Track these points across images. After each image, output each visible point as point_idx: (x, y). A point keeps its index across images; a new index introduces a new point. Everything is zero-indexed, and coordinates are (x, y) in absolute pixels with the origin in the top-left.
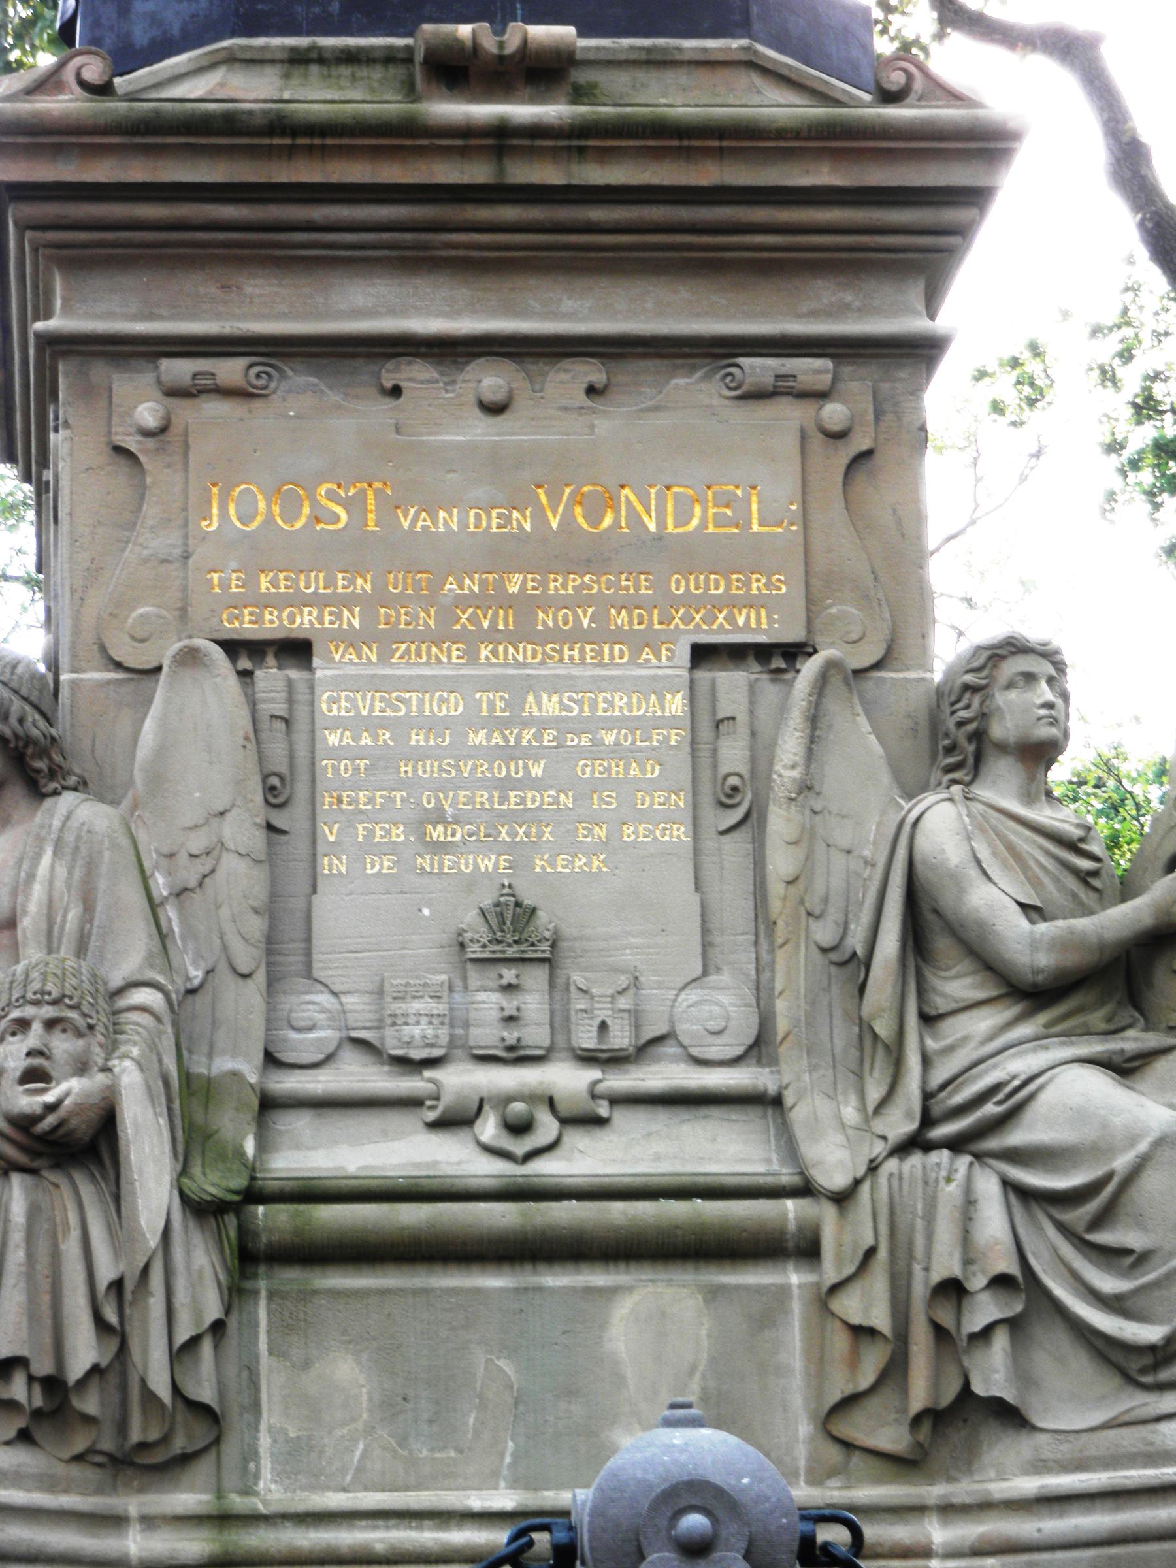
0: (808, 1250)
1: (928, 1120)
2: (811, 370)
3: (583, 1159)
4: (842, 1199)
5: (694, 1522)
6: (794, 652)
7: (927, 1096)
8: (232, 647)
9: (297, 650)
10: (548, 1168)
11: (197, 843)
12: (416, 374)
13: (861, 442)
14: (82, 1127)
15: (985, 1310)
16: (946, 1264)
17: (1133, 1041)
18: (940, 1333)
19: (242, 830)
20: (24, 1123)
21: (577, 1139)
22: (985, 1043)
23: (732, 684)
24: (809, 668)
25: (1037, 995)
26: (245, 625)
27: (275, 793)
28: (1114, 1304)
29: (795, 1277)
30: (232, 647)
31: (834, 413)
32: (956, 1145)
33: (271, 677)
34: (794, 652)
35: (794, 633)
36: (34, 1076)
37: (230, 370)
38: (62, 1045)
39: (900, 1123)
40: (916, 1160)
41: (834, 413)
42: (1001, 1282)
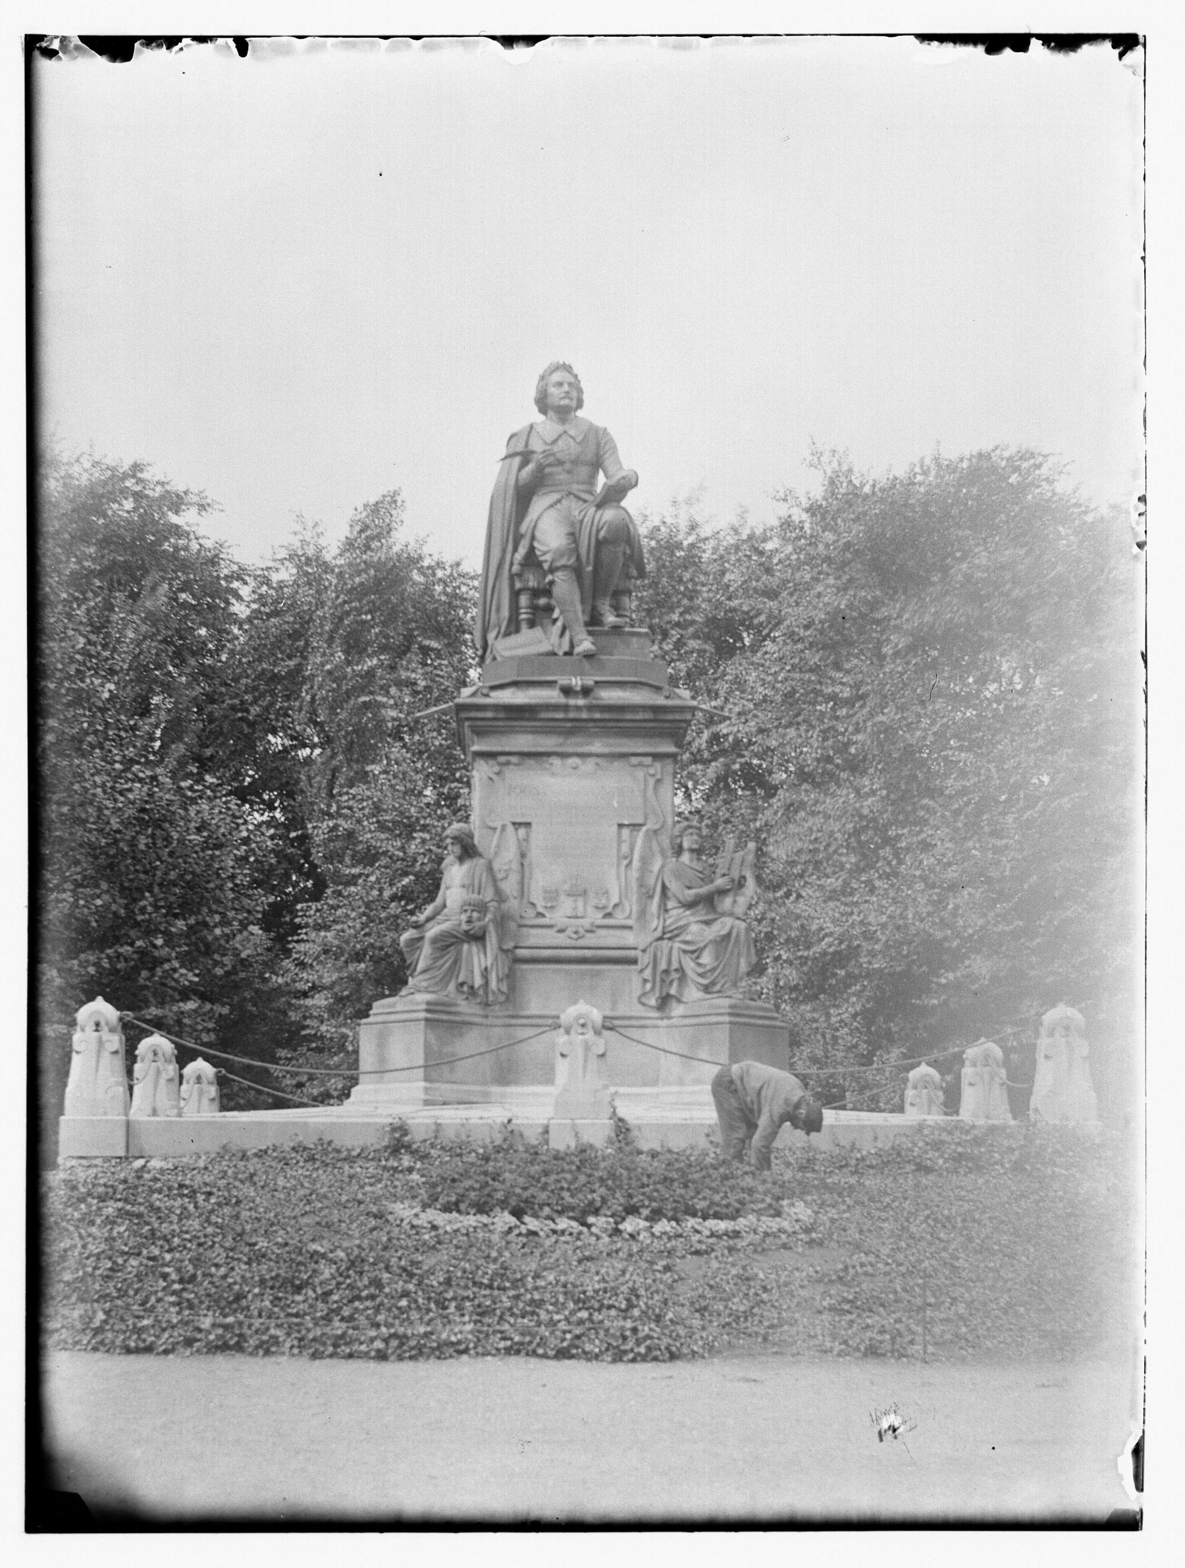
0: (634, 962)
1: (664, 933)
2: (648, 760)
3: (590, 940)
4: (644, 951)
5: (582, 1021)
6: (641, 825)
7: (664, 927)
8: (514, 824)
9: (528, 825)
10: (581, 943)
11: (506, 867)
12: (556, 761)
13: (659, 776)
14: (480, 933)
15: (675, 975)
16: (663, 966)
17: (711, 917)
18: (663, 981)
19: (515, 866)
20: (467, 932)
21: (588, 935)
22: (676, 914)
23: (626, 832)
24: (644, 829)
25: (690, 905)
26: (518, 820)
27: (523, 855)
28: (700, 975)
29: (633, 967)
30: (514, 824)
31: (652, 771)
32: (670, 939)
33: (522, 832)
34: (641, 825)
35: (640, 821)
36: (469, 921)
37: (514, 759)
38: (475, 915)
39: (658, 933)
40: (660, 942)
41: (652, 771)
42: (676, 970)
